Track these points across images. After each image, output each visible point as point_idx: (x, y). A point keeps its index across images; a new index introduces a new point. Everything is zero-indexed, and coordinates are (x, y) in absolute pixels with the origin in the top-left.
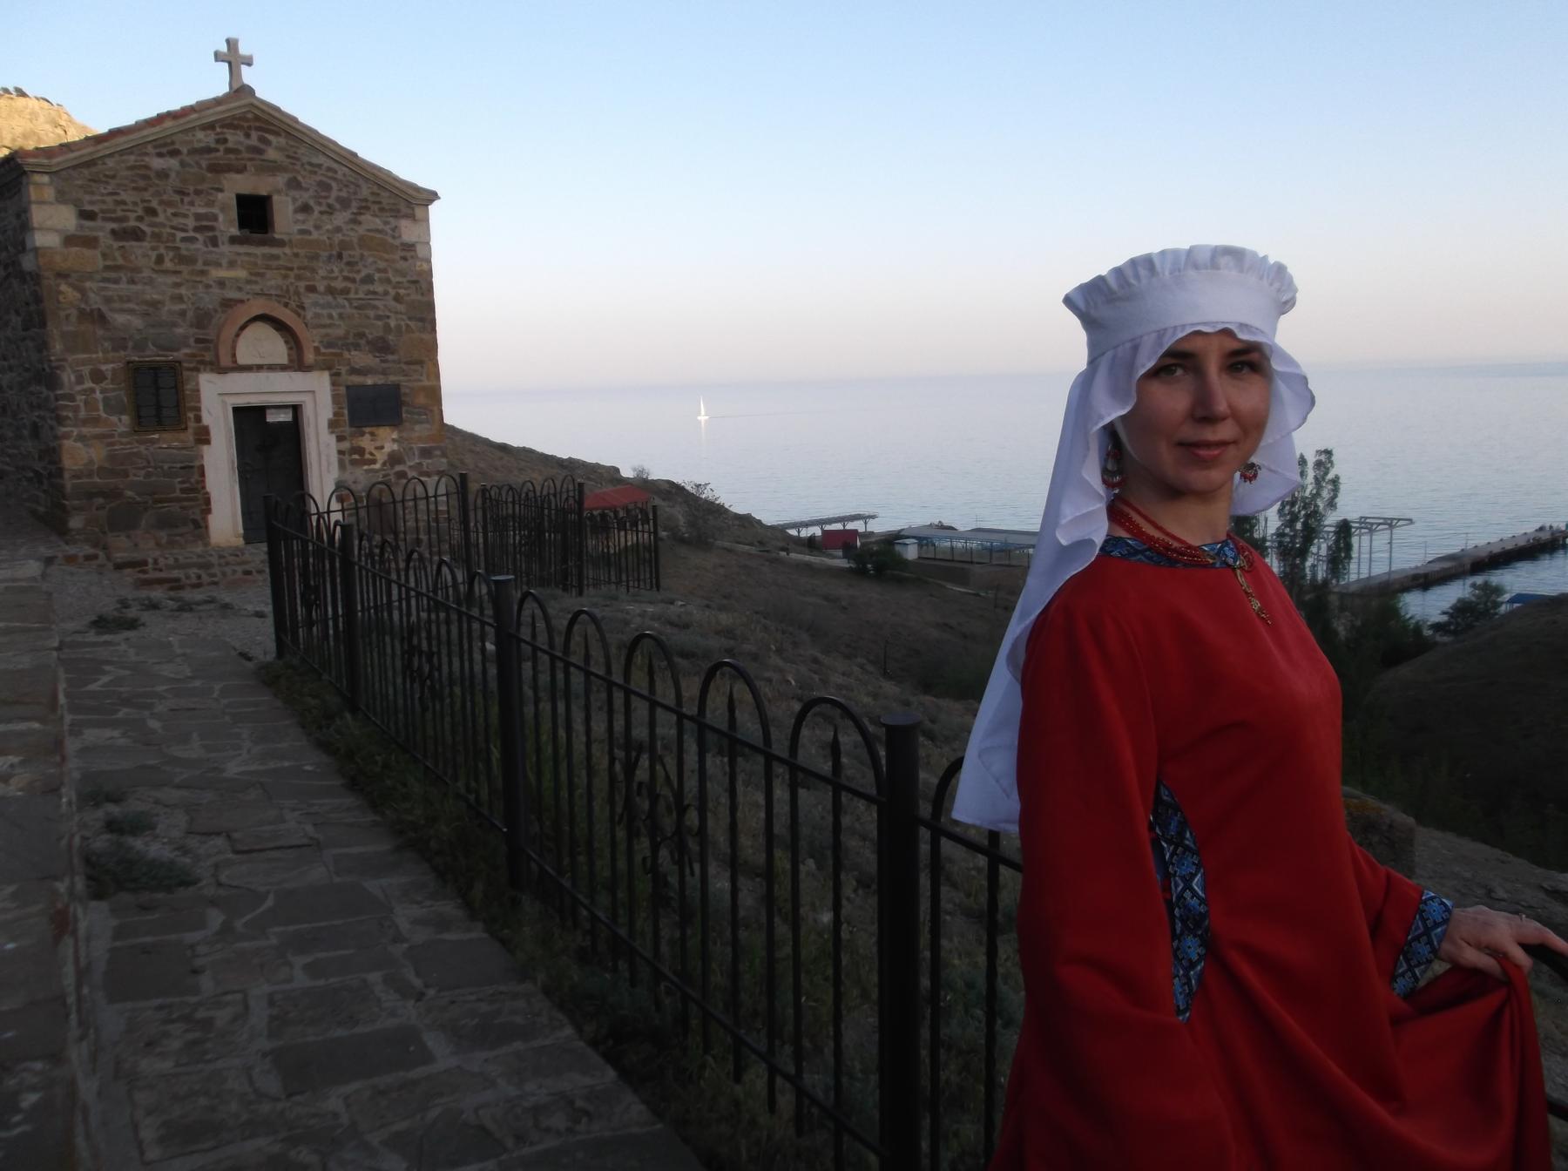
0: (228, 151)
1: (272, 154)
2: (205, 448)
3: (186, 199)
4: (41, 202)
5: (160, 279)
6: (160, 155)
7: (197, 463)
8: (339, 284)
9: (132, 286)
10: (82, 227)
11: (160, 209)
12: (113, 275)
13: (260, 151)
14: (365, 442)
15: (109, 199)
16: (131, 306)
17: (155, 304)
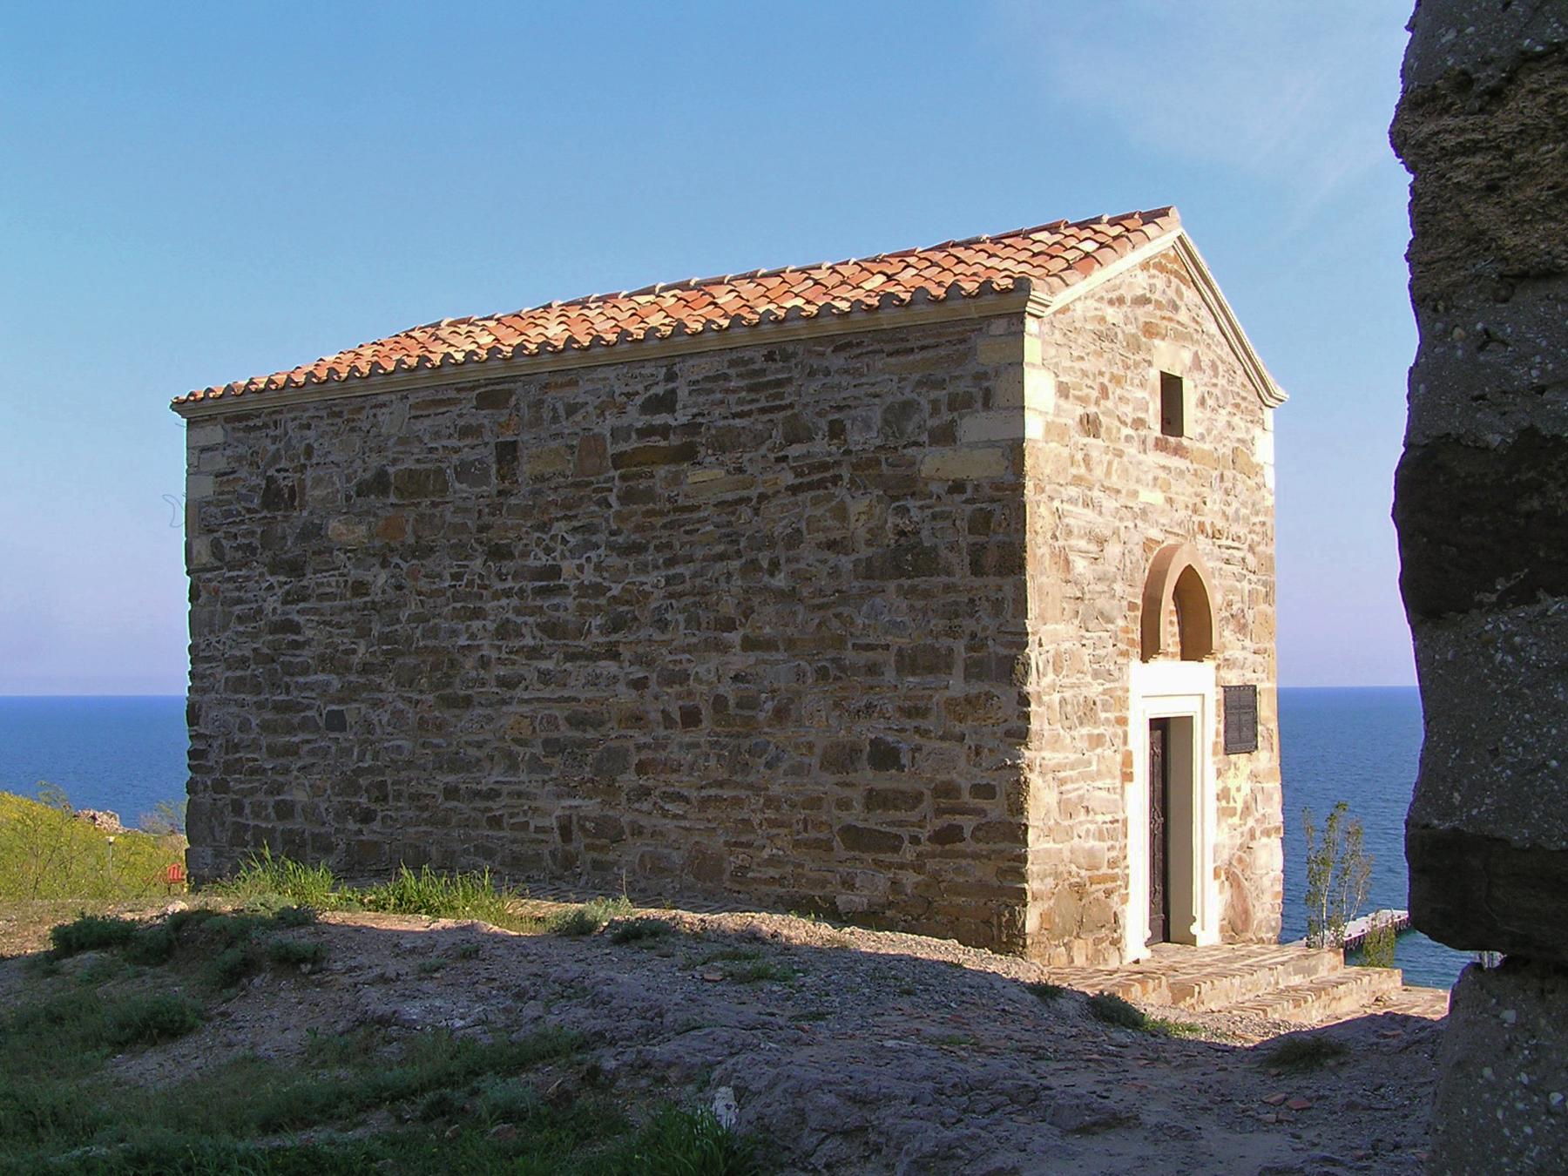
0: (1159, 305)
1: (1183, 316)
2: (1128, 786)
3: (1129, 374)
4: (1033, 365)
5: (1110, 504)
6: (1111, 302)
7: (1120, 816)
8: (1220, 524)
9: (1086, 511)
10: (1057, 407)
11: (1111, 387)
12: (1073, 491)
13: (1176, 308)
14: (1232, 784)
15: (1078, 365)
16: (1082, 544)
17: (1101, 542)
